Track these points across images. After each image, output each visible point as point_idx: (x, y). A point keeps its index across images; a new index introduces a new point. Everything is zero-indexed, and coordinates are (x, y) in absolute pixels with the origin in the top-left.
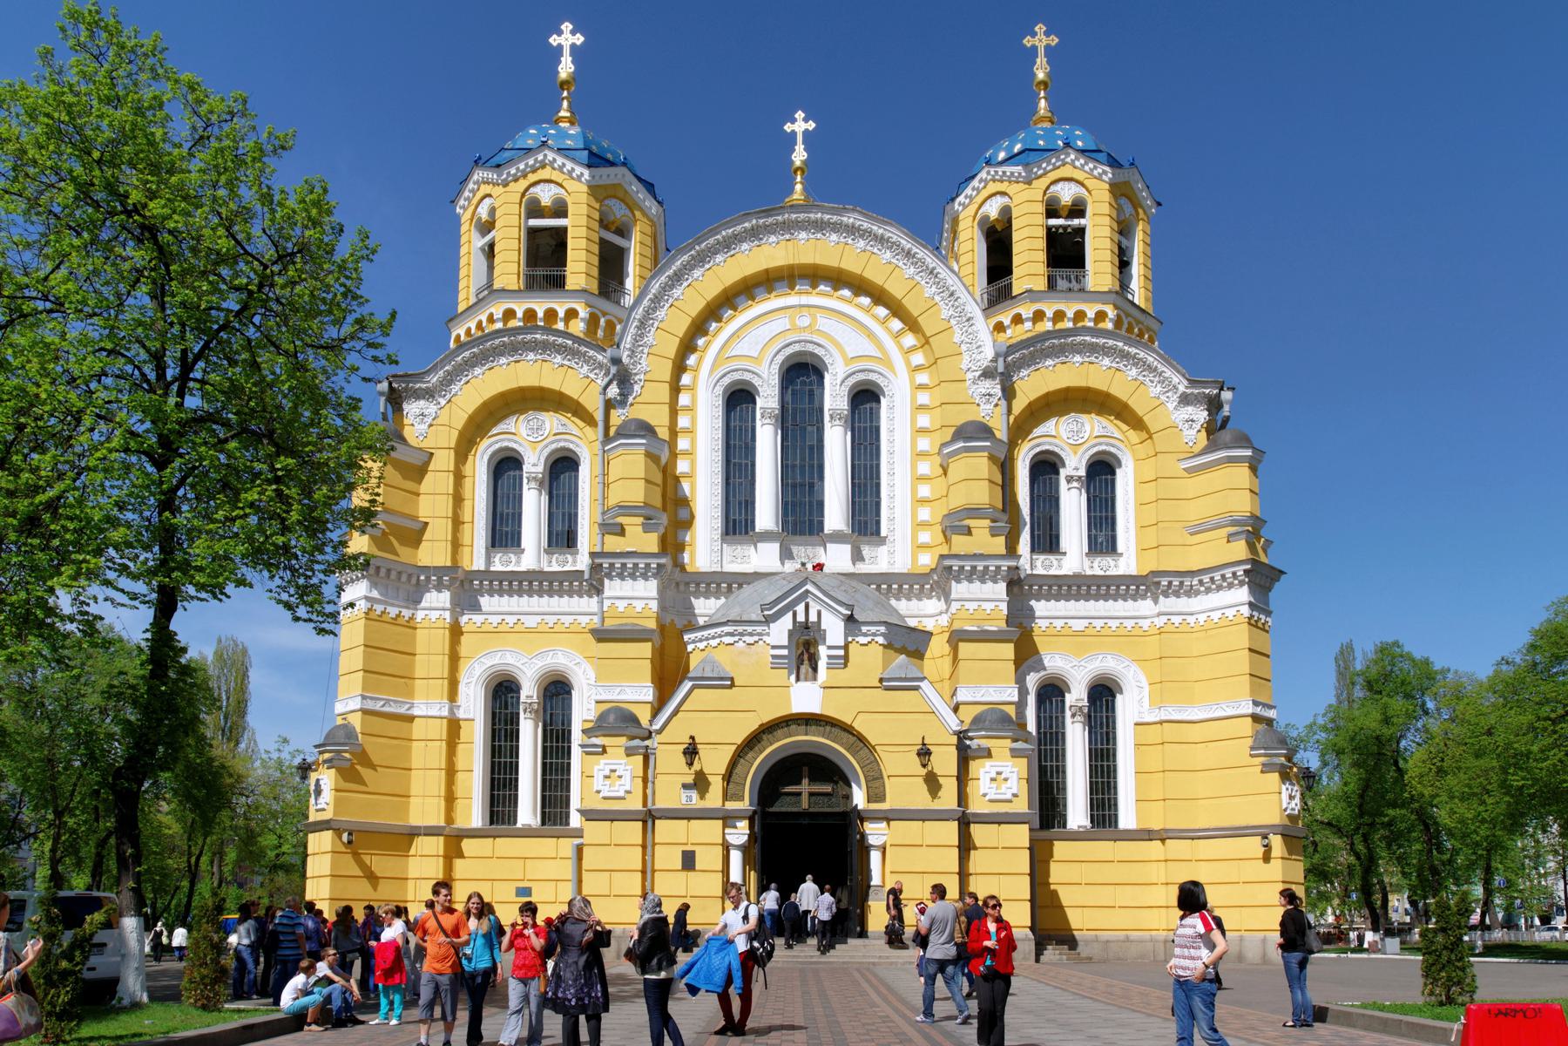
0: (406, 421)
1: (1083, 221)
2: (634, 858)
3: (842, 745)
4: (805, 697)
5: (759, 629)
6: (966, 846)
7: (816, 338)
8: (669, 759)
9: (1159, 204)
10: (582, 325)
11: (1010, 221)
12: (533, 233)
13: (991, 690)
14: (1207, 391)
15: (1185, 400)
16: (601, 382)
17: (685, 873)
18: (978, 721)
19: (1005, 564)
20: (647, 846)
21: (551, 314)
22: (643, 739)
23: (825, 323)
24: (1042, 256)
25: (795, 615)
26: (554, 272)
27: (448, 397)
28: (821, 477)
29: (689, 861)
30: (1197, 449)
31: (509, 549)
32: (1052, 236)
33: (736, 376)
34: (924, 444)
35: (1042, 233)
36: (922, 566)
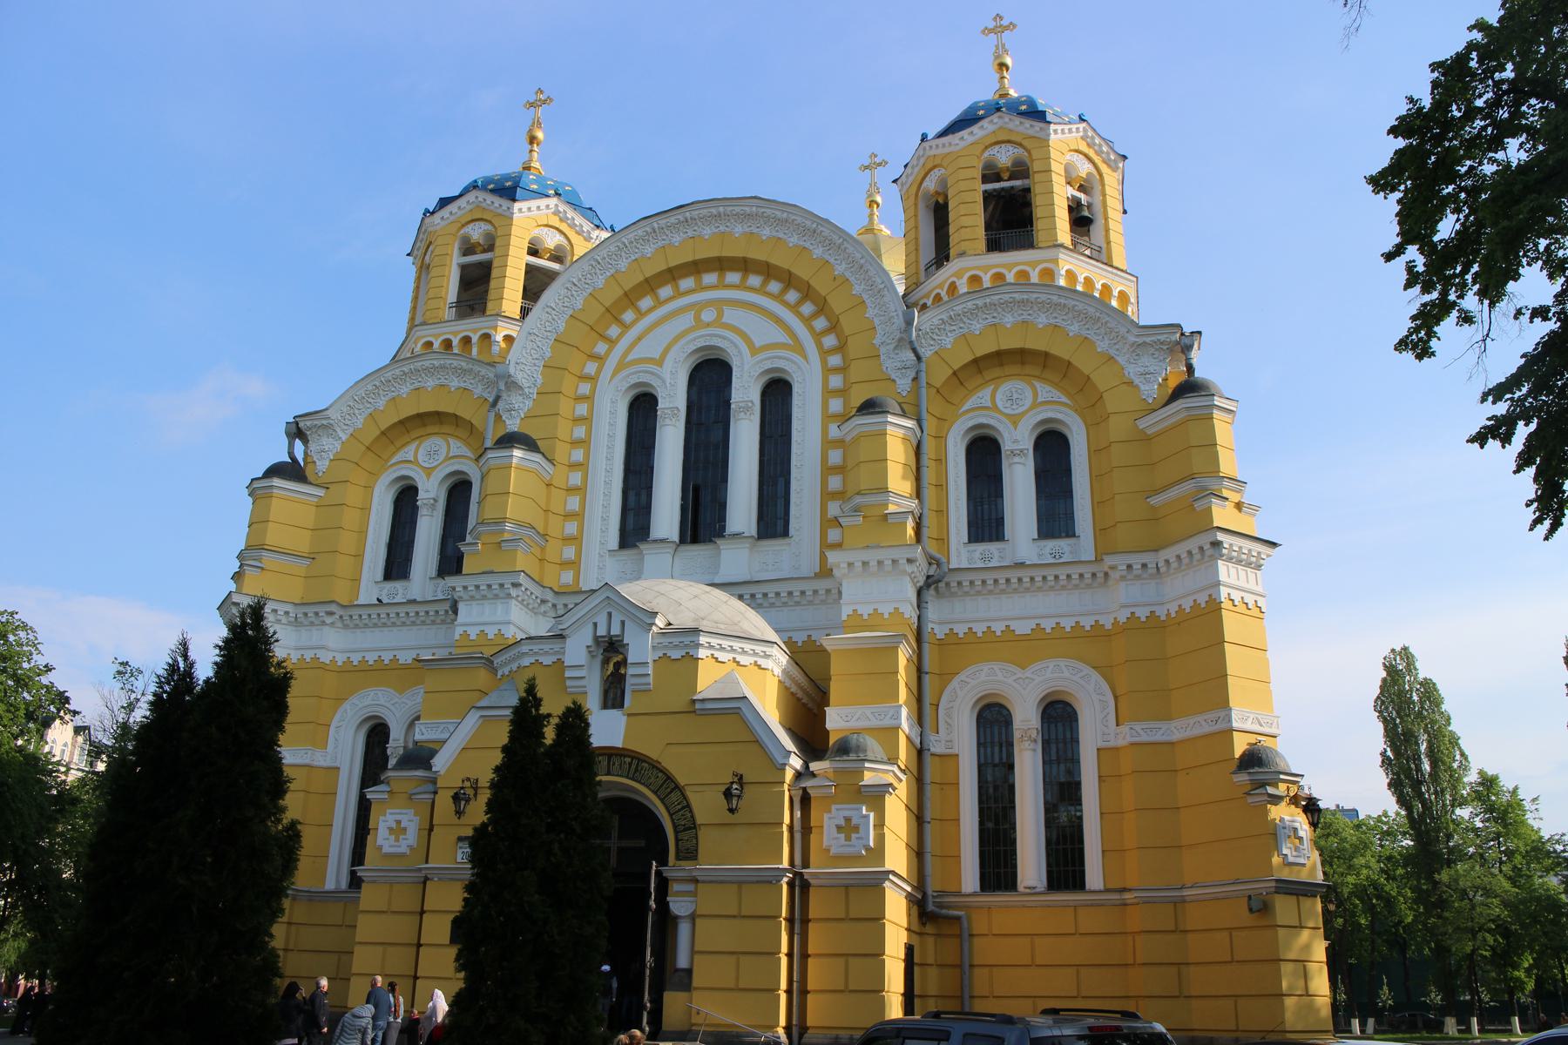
1: (1026, 182)
3: (647, 786)
8: (444, 802)
12: (464, 268)
14: (1162, 338)
16: (491, 400)
21: (467, 341)
25: (595, 625)
28: (725, 480)
32: (987, 196)
33: (634, 380)
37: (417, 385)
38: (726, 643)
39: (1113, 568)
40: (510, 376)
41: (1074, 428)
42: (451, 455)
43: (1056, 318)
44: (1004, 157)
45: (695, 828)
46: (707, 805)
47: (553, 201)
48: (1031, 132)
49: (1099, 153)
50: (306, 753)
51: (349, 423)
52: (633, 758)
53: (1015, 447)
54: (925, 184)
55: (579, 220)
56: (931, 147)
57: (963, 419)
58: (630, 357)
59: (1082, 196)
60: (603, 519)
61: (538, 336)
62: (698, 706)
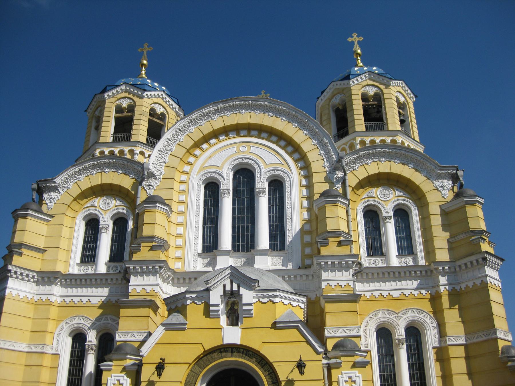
0: (44, 202)
9: (416, 97)
12: (116, 119)
13: (345, 329)
18: (336, 347)
21: (122, 152)
24: (362, 117)
25: (224, 286)
26: (126, 135)
27: (66, 189)
31: (87, 264)
33: (209, 175)
38: (287, 296)
40: (149, 169)
41: (412, 208)
42: (117, 204)
43: (403, 160)
45: (277, 382)
47: (160, 93)
48: (382, 82)
49: (408, 94)
50: (43, 347)
51: (65, 186)
52: (244, 349)
53: (387, 215)
54: (333, 100)
55: (171, 102)
56: (337, 85)
60: (195, 239)
61: (162, 152)
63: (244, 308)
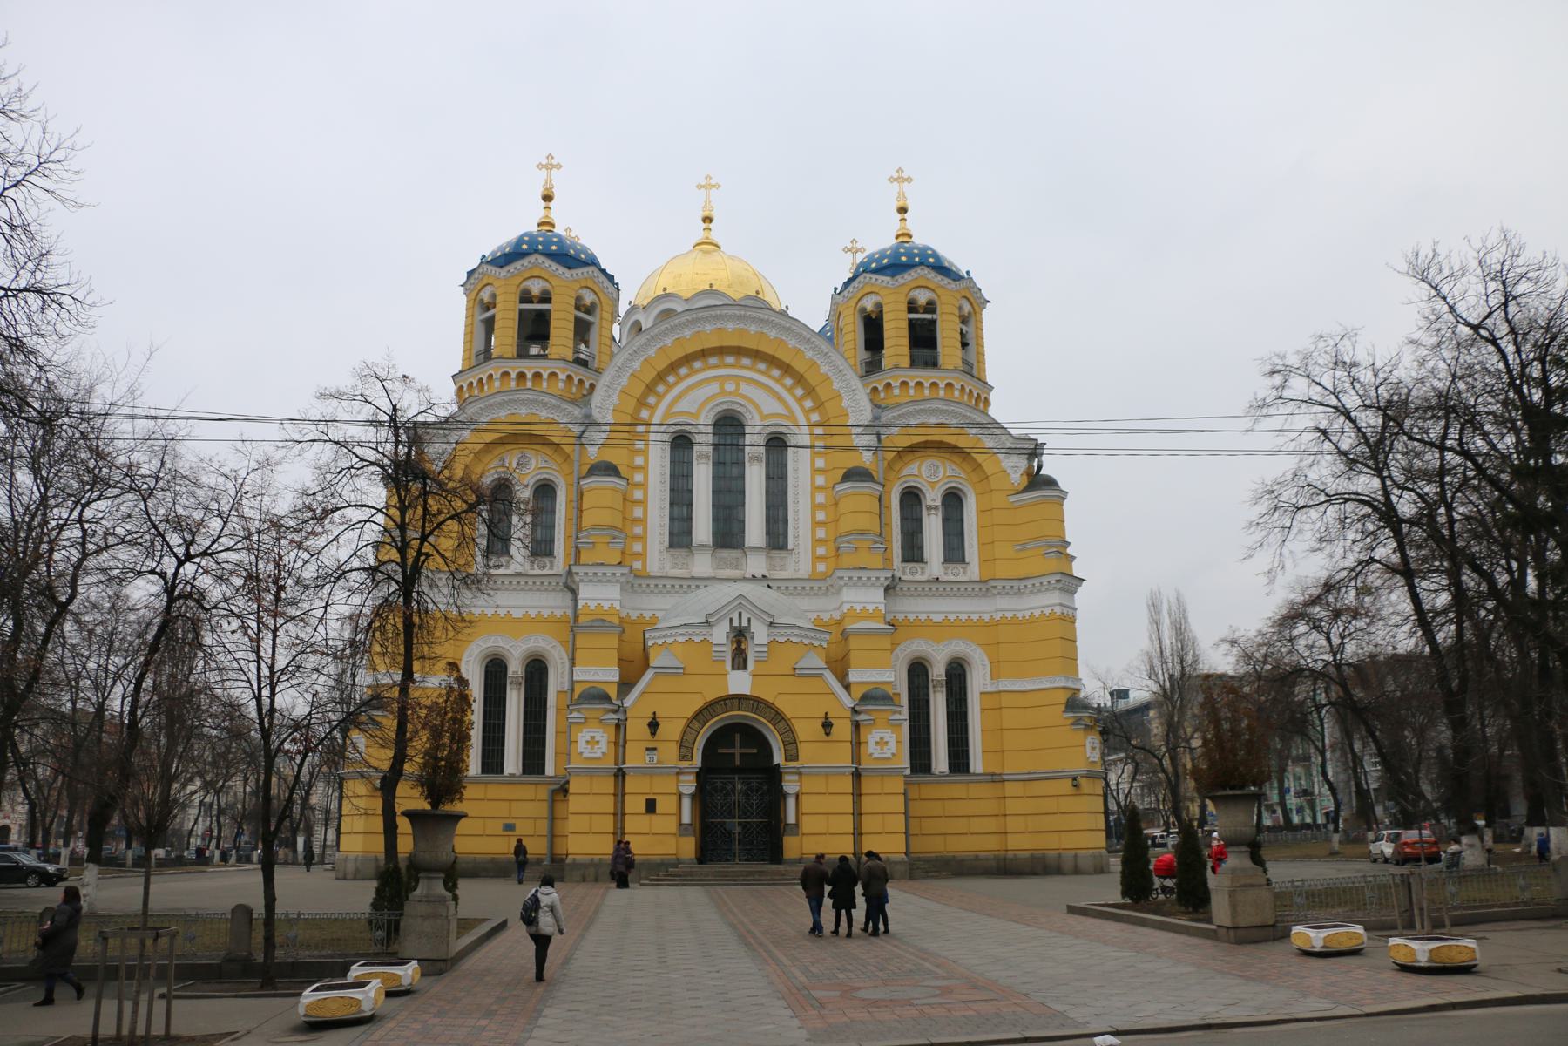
1: (935, 316)
2: (608, 804)
4: (739, 683)
5: (704, 631)
6: (857, 795)
7: (739, 400)
10: (561, 385)
11: (881, 312)
12: (521, 312)
14: (1026, 446)
15: (1010, 451)
17: (648, 817)
18: (865, 698)
19: (883, 575)
20: (620, 795)
21: (537, 375)
22: (615, 712)
23: (746, 389)
24: (906, 341)
25: (731, 620)
29: (651, 806)
30: (1021, 488)
32: (912, 323)
34: (820, 480)
35: (905, 324)
36: (822, 572)
37: (513, 411)
39: (995, 587)
44: (922, 297)
46: (807, 730)
48: (942, 283)
52: (754, 701)
57: (901, 481)
58: (675, 409)
59: (965, 328)
60: (661, 526)
62: (797, 672)
63: (757, 649)
